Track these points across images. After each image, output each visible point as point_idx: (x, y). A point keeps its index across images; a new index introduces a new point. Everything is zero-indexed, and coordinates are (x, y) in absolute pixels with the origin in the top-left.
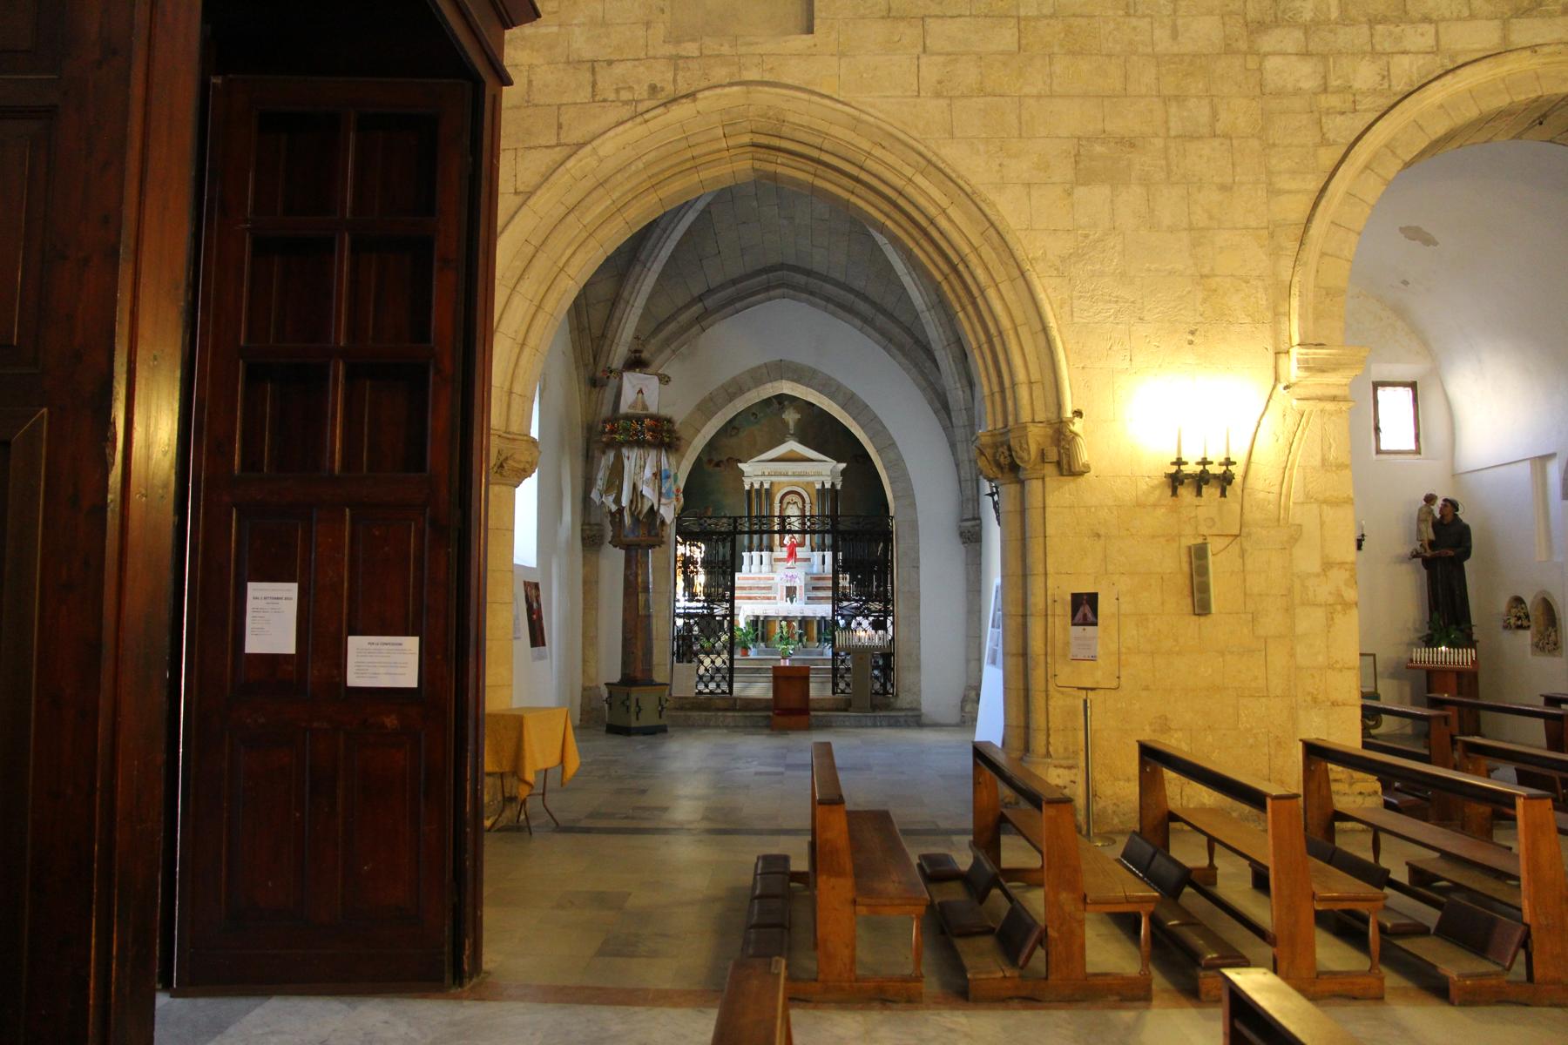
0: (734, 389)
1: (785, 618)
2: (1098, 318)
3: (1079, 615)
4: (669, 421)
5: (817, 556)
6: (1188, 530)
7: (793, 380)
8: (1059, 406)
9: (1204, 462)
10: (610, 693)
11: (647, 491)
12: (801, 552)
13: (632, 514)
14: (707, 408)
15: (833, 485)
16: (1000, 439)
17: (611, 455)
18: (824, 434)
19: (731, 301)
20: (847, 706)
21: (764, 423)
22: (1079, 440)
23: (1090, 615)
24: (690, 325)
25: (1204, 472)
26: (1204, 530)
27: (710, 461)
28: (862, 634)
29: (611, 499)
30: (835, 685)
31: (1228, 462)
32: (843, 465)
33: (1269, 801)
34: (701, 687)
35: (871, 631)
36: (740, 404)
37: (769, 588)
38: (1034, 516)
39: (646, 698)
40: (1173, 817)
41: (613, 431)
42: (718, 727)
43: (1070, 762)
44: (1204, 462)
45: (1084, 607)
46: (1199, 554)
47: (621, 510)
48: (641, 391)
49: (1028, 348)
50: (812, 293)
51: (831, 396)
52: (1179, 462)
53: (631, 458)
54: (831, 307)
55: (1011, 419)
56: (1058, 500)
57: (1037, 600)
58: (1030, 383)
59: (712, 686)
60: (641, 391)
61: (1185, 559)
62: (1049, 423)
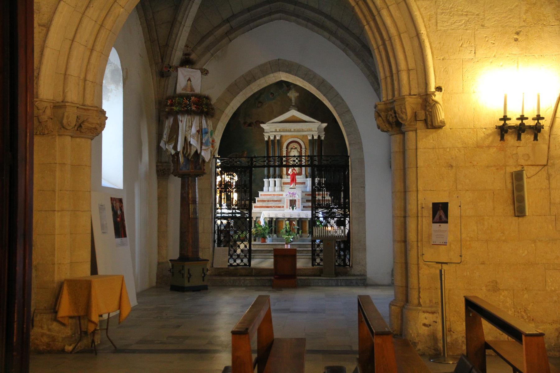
0: (250, 78)
1: (289, 219)
2: (454, 26)
3: (437, 217)
4: (207, 98)
6: (511, 162)
7: (286, 72)
8: (427, 84)
9: (522, 118)
10: (173, 266)
11: (193, 142)
12: (299, 179)
13: (184, 156)
14: (233, 90)
15: (319, 137)
16: (390, 106)
17: (171, 120)
18: (312, 107)
19: (247, 22)
20: (320, 273)
21: (274, 98)
22: (438, 106)
23: (443, 217)
24: (222, 37)
25: (522, 124)
26: (522, 162)
27: (245, 123)
28: (329, 228)
29: (171, 146)
30: (314, 260)
31: (539, 118)
32: (325, 125)
33: (523, 337)
34: (231, 261)
35: (335, 227)
36: (254, 88)
37: (280, 201)
38: (410, 153)
39: (195, 269)
40: (487, 346)
41: (172, 105)
42: (240, 286)
43: (433, 309)
44: (522, 118)
45: (440, 212)
46: (518, 177)
47: (177, 153)
48: (189, 80)
49: (408, 47)
50: (298, 16)
51: (310, 81)
52: (505, 118)
53: (184, 121)
54: (310, 24)
55: (396, 93)
56: (425, 143)
57: (412, 207)
58: (409, 70)
59: (238, 261)
60: (189, 80)
61: (509, 180)
62: (419, 95)
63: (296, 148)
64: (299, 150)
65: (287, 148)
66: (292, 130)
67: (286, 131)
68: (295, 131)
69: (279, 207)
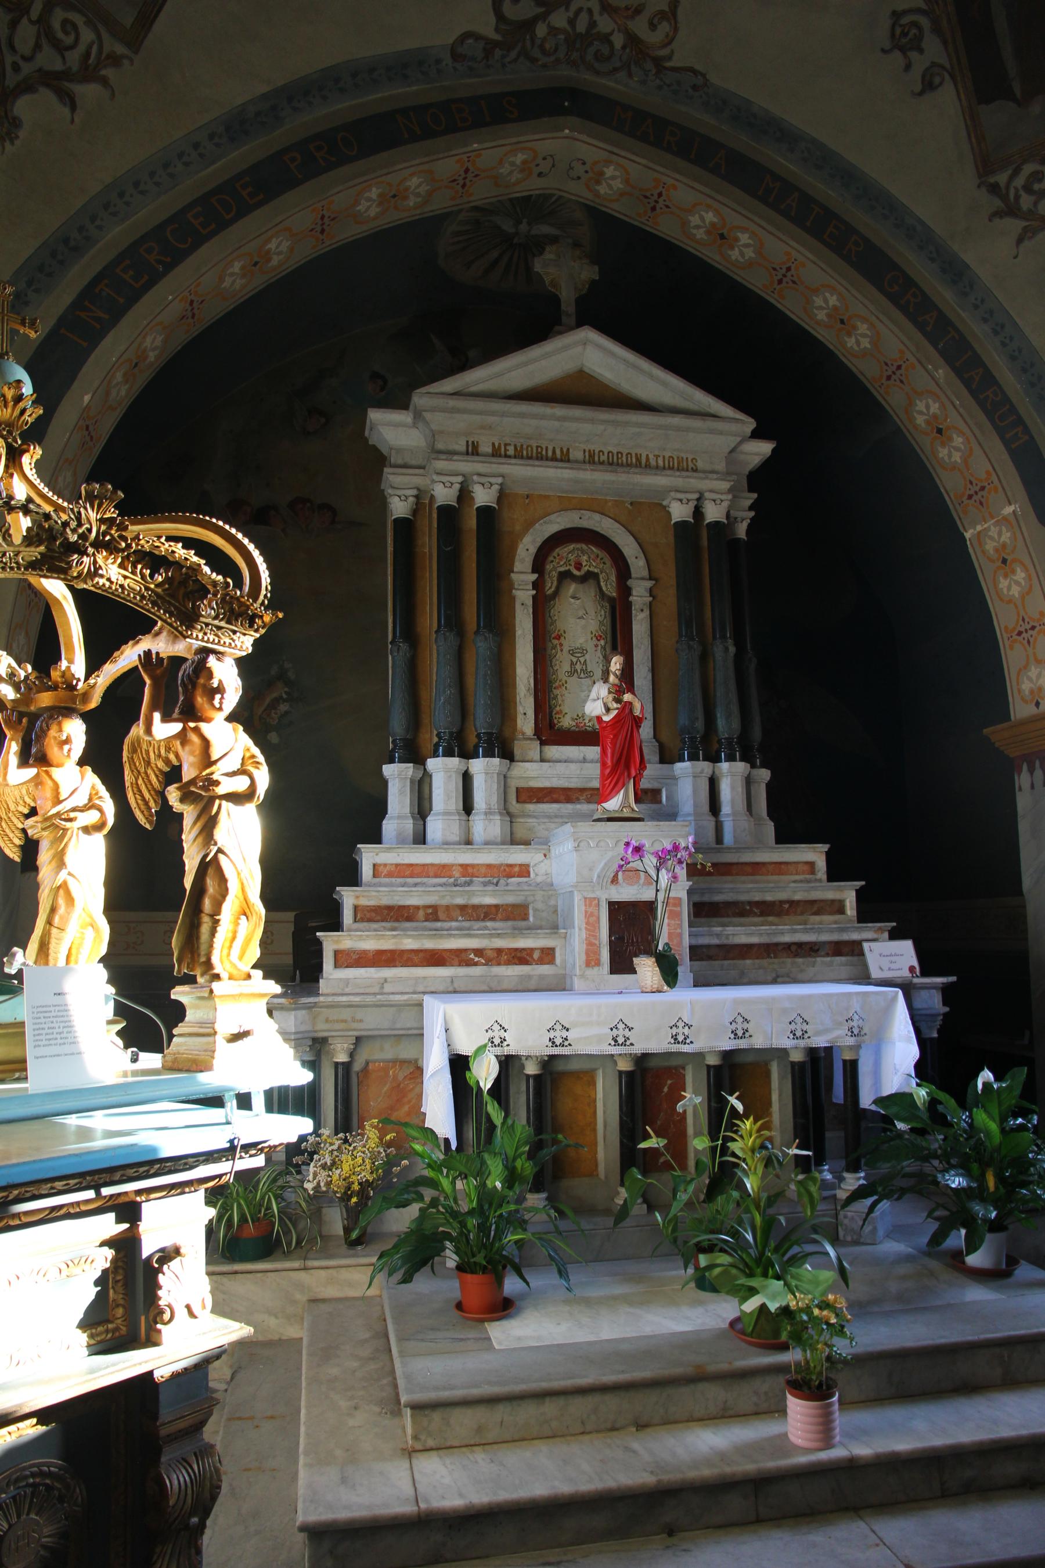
5: (687, 778)
63: (590, 577)
64: (610, 587)
65: (539, 565)
66: (576, 454)
67: (540, 456)
68: (591, 460)
69: (520, 957)
